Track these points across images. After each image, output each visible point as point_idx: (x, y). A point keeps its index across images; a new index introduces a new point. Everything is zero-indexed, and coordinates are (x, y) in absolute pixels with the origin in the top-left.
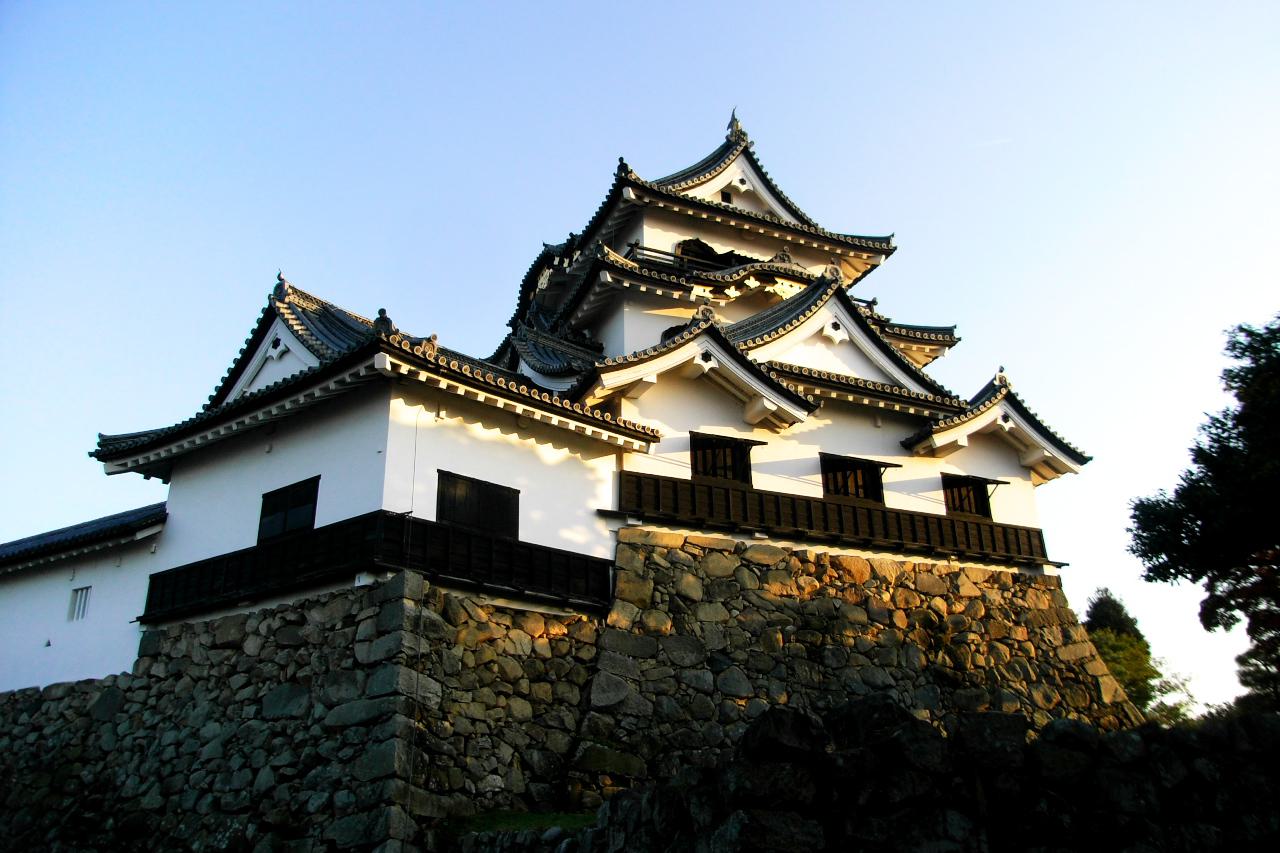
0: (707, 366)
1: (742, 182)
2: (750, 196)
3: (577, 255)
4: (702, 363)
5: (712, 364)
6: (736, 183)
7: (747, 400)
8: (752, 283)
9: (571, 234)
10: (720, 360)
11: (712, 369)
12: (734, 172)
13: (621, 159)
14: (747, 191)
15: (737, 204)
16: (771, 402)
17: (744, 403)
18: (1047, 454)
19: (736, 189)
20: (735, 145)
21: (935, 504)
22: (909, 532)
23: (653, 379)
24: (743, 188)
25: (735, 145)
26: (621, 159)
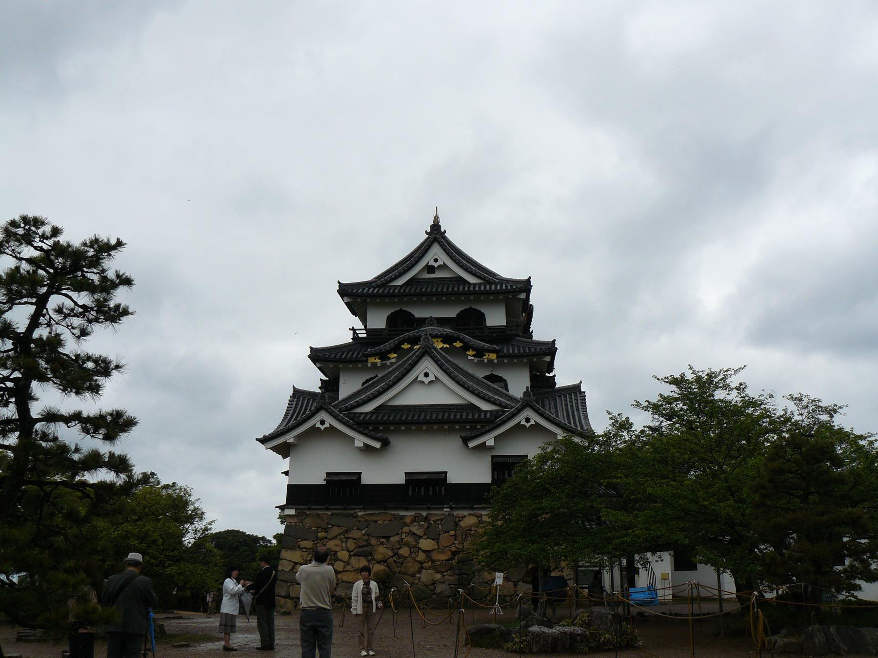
0: (322, 427)
1: (436, 260)
2: (444, 267)
4: (320, 426)
5: (327, 425)
6: (432, 263)
10: (330, 421)
11: (326, 428)
12: (436, 254)
14: (439, 266)
15: (437, 275)
16: (360, 441)
18: (559, 438)
19: (432, 266)
20: (436, 235)
21: (485, 477)
22: (469, 495)
23: (292, 440)
25: (436, 235)
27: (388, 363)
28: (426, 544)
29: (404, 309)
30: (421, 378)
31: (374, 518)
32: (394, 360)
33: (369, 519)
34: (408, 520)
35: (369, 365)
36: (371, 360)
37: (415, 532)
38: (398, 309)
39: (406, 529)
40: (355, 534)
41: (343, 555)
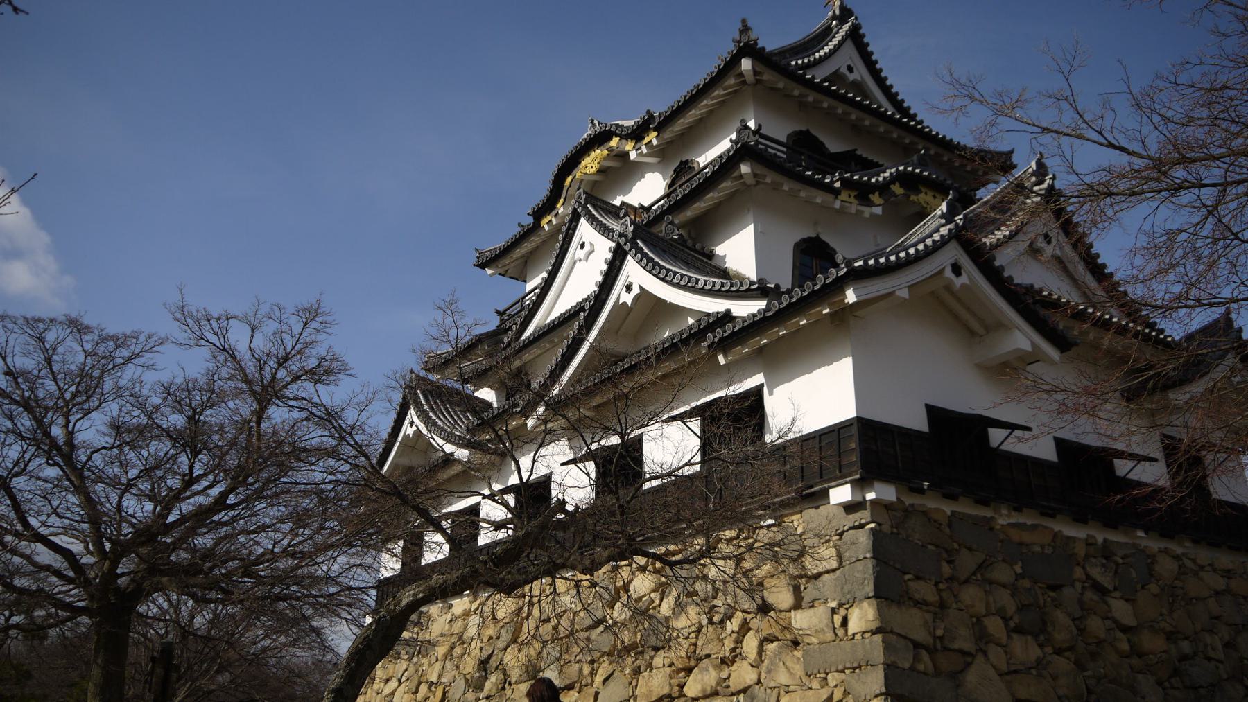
0: (959, 282)
1: (850, 69)
2: (858, 87)
3: (652, 137)
4: (952, 276)
6: (844, 70)
7: (981, 331)
8: (897, 189)
9: (648, 112)
11: (963, 285)
13: (744, 21)
16: (1022, 338)
17: (972, 333)
24: (851, 77)
26: (744, 21)
27: (867, 211)
28: (1121, 609)
29: (814, 132)
30: (1041, 243)
31: (1026, 537)
32: (878, 210)
33: (1015, 535)
34: (1081, 550)
35: (837, 205)
36: (844, 196)
37: (1099, 578)
38: (804, 129)
39: (1078, 573)
40: (1002, 573)
41: (994, 625)
